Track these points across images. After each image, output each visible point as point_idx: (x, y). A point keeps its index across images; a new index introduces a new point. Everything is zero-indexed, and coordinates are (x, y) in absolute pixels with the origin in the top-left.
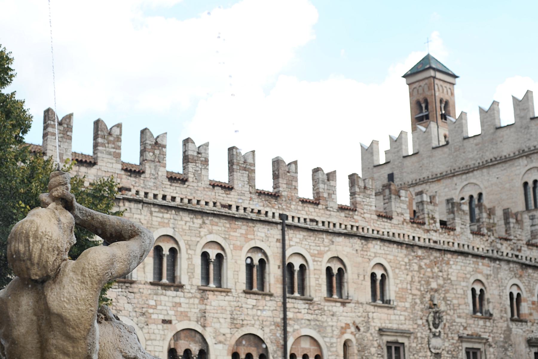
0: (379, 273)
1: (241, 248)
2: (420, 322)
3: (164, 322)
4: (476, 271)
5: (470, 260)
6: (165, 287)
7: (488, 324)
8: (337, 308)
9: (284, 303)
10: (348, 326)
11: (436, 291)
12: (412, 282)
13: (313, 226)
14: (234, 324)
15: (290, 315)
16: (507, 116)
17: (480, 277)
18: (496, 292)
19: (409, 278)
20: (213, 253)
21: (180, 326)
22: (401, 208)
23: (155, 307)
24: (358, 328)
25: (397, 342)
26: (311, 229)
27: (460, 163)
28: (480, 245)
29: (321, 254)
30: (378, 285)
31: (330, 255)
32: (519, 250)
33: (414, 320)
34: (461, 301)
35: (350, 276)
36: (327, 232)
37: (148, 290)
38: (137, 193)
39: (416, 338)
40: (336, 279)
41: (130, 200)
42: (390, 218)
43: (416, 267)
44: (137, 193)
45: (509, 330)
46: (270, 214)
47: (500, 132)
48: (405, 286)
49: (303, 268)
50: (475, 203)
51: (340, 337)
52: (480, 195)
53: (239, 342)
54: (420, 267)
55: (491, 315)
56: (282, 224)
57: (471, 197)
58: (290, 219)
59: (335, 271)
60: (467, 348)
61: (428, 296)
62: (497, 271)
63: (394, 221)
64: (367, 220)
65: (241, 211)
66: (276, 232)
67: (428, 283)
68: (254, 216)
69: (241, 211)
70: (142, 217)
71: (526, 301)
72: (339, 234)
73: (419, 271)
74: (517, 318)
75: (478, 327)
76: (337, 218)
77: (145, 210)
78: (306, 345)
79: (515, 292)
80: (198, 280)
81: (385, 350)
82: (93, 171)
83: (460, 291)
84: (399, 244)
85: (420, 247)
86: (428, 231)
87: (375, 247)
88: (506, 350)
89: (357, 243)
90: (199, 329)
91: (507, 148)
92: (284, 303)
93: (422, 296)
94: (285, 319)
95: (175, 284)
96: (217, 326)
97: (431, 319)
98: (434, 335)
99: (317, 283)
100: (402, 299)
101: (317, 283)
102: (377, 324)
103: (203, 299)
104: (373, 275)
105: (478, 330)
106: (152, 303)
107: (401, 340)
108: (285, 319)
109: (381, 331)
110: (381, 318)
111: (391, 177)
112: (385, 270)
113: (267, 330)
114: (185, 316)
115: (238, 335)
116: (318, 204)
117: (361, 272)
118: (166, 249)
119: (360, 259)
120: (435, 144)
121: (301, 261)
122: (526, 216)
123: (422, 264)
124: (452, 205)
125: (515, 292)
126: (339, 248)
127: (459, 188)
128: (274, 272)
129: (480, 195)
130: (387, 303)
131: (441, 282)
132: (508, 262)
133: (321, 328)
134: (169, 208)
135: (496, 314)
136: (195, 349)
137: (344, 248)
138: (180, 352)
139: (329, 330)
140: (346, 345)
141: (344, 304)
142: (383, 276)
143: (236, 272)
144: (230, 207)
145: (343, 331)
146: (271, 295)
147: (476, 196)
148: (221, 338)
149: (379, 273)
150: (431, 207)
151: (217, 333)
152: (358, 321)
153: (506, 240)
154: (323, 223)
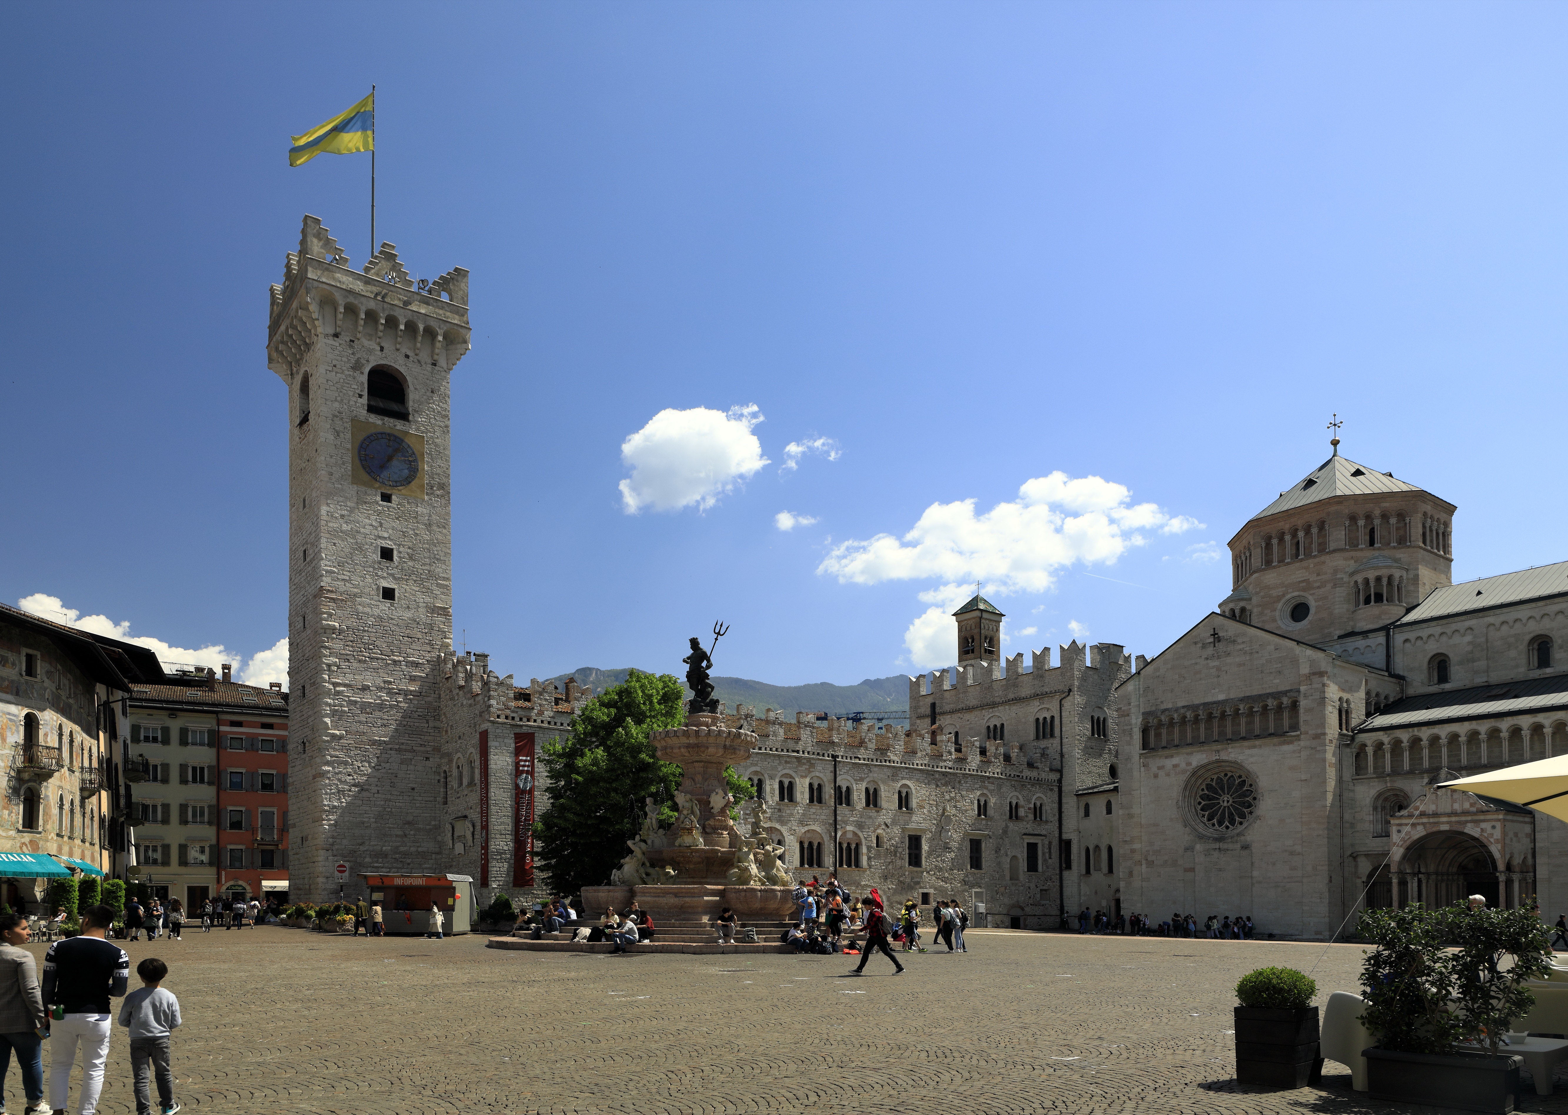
147: (998, 725)
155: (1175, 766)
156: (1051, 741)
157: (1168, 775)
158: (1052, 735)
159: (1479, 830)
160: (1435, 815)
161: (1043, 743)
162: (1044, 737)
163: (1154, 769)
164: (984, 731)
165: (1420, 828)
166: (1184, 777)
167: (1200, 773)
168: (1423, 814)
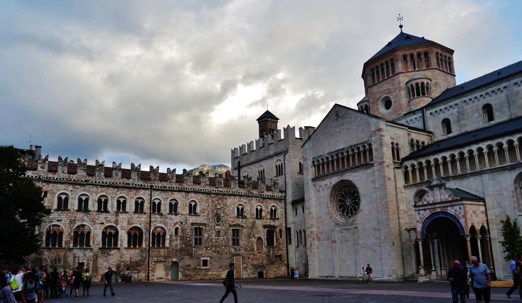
0: (193, 204)
1: (133, 198)
3: (101, 223)
4: (240, 201)
5: (237, 197)
6: (102, 212)
7: (244, 220)
8: (173, 217)
9: (150, 216)
10: (177, 223)
11: (220, 209)
12: (208, 206)
13: (165, 189)
14: (129, 223)
15: (152, 219)
17: (241, 203)
18: (249, 208)
19: (207, 205)
20: (122, 200)
21: (107, 225)
23: (98, 219)
24: (182, 223)
26: (164, 190)
27: (258, 158)
29: (167, 198)
31: (171, 198)
32: (263, 193)
33: (208, 220)
36: (170, 191)
37: (95, 213)
38: (92, 182)
39: (209, 226)
41: (89, 184)
42: (200, 184)
43: (211, 201)
44: (92, 182)
45: (255, 222)
46: (146, 186)
48: (205, 208)
49: (159, 204)
51: (173, 226)
53: (131, 229)
54: (213, 201)
55: (246, 217)
56: (151, 189)
58: (155, 187)
65: (134, 185)
66: (148, 192)
67: (216, 206)
68: (139, 187)
69: (134, 185)
70: (94, 190)
72: (175, 191)
73: (212, 202)
75: (239, 221)
77: (95, 188)
78: (159, 229)
79: (259, 208)
80: (115, 209)
81: (194, 231)
82: (75, 176)
84: (203, 193)
85: (213, 194)
86: (217, 188)
88: (253, 229)
89: (184, 194)
90: (115, 225)
92: (150, 216)
93: (213, 211)
94: (150, 221)
95: (106, 211)
96: (122, 224)
98: (217, 225)
99: (165, 209)
100: (204, 212)
101: (165, 209)
103: (117, 216)
106: (97, 217)
107: (201, 227)
108: (150, 221)
109: (193, 224)
110: (192, 219)
111: (239, 162)
113: (142, 225)
114: (109, 221)
115: (130, 227)
116: (167, 181)
117: (185, 204)
118: (103, 199)
119: (184, 199)
121: (159, 201)
123: (214, 200)
125: (259, 208)
126: (175, 196)
128: (147, 205)
130: (196, 214)
132: (256, 197)
133: (166, 224)
134: (104, 186)
135: (248, 216)
136: (113, 232)
137: (177, 196)
138: (107, 233)
139: (169, 224)
140: (177, 229)
141: (176, 215)
143: (131, 206)
144: (129, 184)
145: (175, 224)
146: (145, 213)
148: (124, 228)
149: (193, 204)
150: (220, 179)
151: (122, 226)
152: (182, 221)
154: (169, 187)
155: (326, 185)
157: (323, 190)
158: (282, 174)
159: (454, 211)
160: (434, 204)
162: (280, 175)
163: (318, 187)
164: (258, 173)
165: (428, 211)
166: (329, 191)
167: (336, 188)
168: (429, 204)
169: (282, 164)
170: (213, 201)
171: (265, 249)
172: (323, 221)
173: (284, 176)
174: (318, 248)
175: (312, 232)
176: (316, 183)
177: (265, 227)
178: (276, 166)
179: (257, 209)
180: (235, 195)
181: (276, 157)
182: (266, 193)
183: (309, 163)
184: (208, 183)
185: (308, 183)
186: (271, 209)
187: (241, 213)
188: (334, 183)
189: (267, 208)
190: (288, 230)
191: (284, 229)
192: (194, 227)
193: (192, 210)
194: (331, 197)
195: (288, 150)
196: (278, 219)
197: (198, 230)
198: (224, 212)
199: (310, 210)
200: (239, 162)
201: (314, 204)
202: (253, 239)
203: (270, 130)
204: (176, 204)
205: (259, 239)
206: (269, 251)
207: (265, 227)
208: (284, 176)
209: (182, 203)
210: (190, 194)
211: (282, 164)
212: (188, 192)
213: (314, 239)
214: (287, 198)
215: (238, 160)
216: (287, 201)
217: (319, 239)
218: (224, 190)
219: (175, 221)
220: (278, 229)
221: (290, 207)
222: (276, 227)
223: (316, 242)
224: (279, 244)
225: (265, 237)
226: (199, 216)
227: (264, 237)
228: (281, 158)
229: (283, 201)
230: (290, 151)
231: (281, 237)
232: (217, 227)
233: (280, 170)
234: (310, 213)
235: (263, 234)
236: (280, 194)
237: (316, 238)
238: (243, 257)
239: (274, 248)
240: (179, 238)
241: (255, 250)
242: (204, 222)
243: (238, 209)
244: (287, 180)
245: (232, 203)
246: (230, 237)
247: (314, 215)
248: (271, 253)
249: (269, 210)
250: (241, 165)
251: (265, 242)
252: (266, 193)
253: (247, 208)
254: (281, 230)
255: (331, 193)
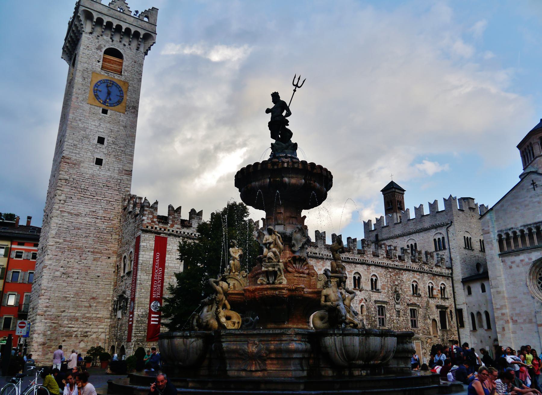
0: (374, 278)
2: (391, 298)
4: (414, 277)
5: (411, 273)
10: (362, 299)
11: (397, 285)
13: (348, 260)
16: (426, 211)
17: (415, 280)
18: (422, 286)
19: (386, 280)
22: (382, 252)
24: (366, 300)
25: (382, 306)
27: (406, 231)
28: (415, 266)
29: (351, 271)
30: (374, 284)
32: (432, 268)
33: (389, 298)
34: (408, 289)
35: (363, 279)
36: (353, 263)
40: (357, 281)
42: (378, 256)
43: (389, 276)
45: (428, 301)
47: (424, 218)
50: (413, 248)
51: (359, 304)
52: (415, 244)
54: (391, 276)
57: (412, 245)
59: (357, 278)
60: (411, 309)
61: (394, 287)
62: (423, 277)
63: (380, 258)
64: (369, 258)
67: (394, 282)
69: (321, 255)
71: (435, 289)
74: (432, 296)
75: (415, 300)
76: (357, 257)
79: (431, 285)
81: (377, 309)
83: (407, 286)
84: (382, 267)
85: (391, 268)
86: (393, 261)
87: (372, 268)
89: (365, 267)
91: (427, 225)
93: (392, 288)
97: (395, 297)
98: (397, 304)
100: (384, 289)
102: (374, 299)
104: (372, 279)
105: (415, 301)
107: (383, 305)
109: (376, 302)
110: (375, 296)
111: (377, 236)
112: (377, 277)
119: (366, 273)
120: (395, 222)
122: (435, 253)
124: (403, 250)
125: (431, 285)
126: (358, 269)
127: (406, 241)
129: (415, 244)
130: (378, 291)
131: (399, 282)
132: (427, 273)
135: (423, 295)
137: (360, 269)
140: (362, 306)
141: (360, 291)
142: (376, 279)
144: (316, 253)
145: (361, 301)
147: (413, 244)
149: (374, 278)
150: (394, 251)
153: (426, 264)
155: (522, 261)
156: (444, 251)
157: (518, 266)
158: (445, 248)
161: (441, 253)
162: (440, 250)
166: (528, 268)
167: (537, 264)
169: (443, 238)
170: (391, 276)
171: (439, 333)
172: (520, 302)
173: (447, 251)
174: (514, 332)
175: (503, 314)
176: (506, 259)
177: (438, 307)
178: (435, 240)
179: (429, 287)
180: (409, 270)
181: (434, 230)
182: (435, 269)
183: (494, 236)
184: (385, 256)
185: (492, 259)
186: (441, 287)
187: (415, 289)
188: (534, 259)
189: (437, 286)
190: (459, 312)
191: (453, 311)
192: (377, 305)
193: (374, 284)
194: (530, 274)
195: (452, 222)
196: (448, 299)
197: (381, 310)
198: (401, 289)
199: (499, 289)
200: (377, 236)
201: (504, 282)
202: (429, 320)
203: (398, 201)
204: (359, 278)
205: (434, 320)
206: (443, 336)
207: (438, 307)
208: (447, 251)
209: (365, 277)
210: (371, 267)
211: (443, 238)
212: (369, 265)
213: (507, 322)
214: (454, 275)
215: (374, 234)
216: (454, 278)
217: (515, 322)
218: (399, 264)
219: (361, 297)
220: (448, 310)
221: (459, 287)
222: (447, 308)
223: (511, 325)
224: (451, 327)
225: (439, 318)
226: (380, 292)
227: (438, 319)
228: (443, 231)
229: (450, 279)
230: (455, 223)
231: (452, 319)
232: (397, 306)
233: (440, 245)
234: (498, 292)
235: (436, 315)
236: (447, 271)
237: (510, 321)
238: (422, 342)
239: (447, 331)
240: (365, 317)
241: (432, 333)
242: (385, 300)
243: (413, 285)
244: (452, 256)
245: (408, 279)
246: (409, 318)
247: (506, 295)
248: (445, 337)
249: (440, 288)
250: (380, 238)
251: (439, 324)
252: (435, 269)
253: (421, 286)
254: (451, 311)
255: (531, 270)
